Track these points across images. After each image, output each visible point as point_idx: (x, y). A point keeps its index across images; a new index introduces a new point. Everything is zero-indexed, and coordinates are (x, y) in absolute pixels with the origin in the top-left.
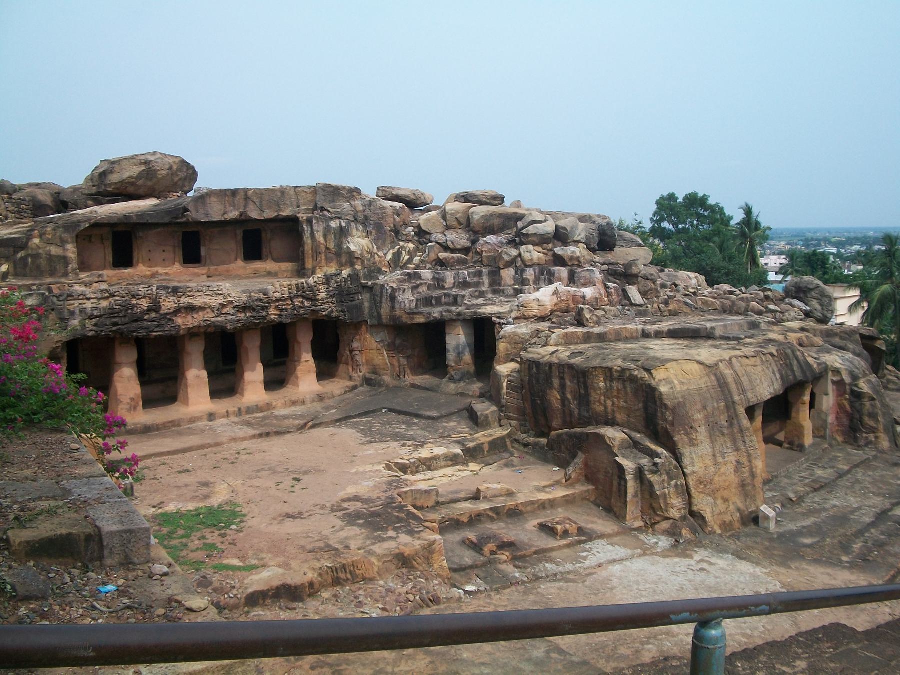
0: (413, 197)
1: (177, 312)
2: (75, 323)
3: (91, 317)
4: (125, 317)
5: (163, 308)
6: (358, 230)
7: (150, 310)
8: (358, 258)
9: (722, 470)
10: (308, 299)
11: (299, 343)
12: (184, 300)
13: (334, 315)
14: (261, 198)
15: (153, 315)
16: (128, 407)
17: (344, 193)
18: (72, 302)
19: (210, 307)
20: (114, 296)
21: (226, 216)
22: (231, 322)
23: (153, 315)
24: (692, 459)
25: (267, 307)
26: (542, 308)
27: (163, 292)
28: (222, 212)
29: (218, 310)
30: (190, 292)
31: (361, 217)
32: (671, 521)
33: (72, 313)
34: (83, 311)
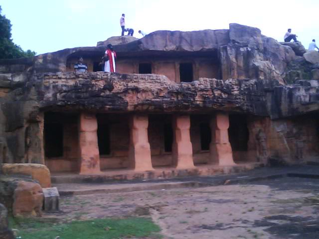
1: (126, 91)
4: (86, 92)
5: (115, 88)
6: (260, 56)
7: (105, 89)
10: (225, 93)
11: (219, 129)
12: (130, 84)
15: (108, 93)
16: (89, 164)
18: (48, 80)
19: (151, 91)
20: (79, 77)
21: (167, 48)
22: (167, 102)
23: (108, 93)
27: (116, 78)
28: (164, 45)
29: (157, 93)
30: (136, 79)
31: (262, 48)
33: (47, 88)
34: (55, 87)
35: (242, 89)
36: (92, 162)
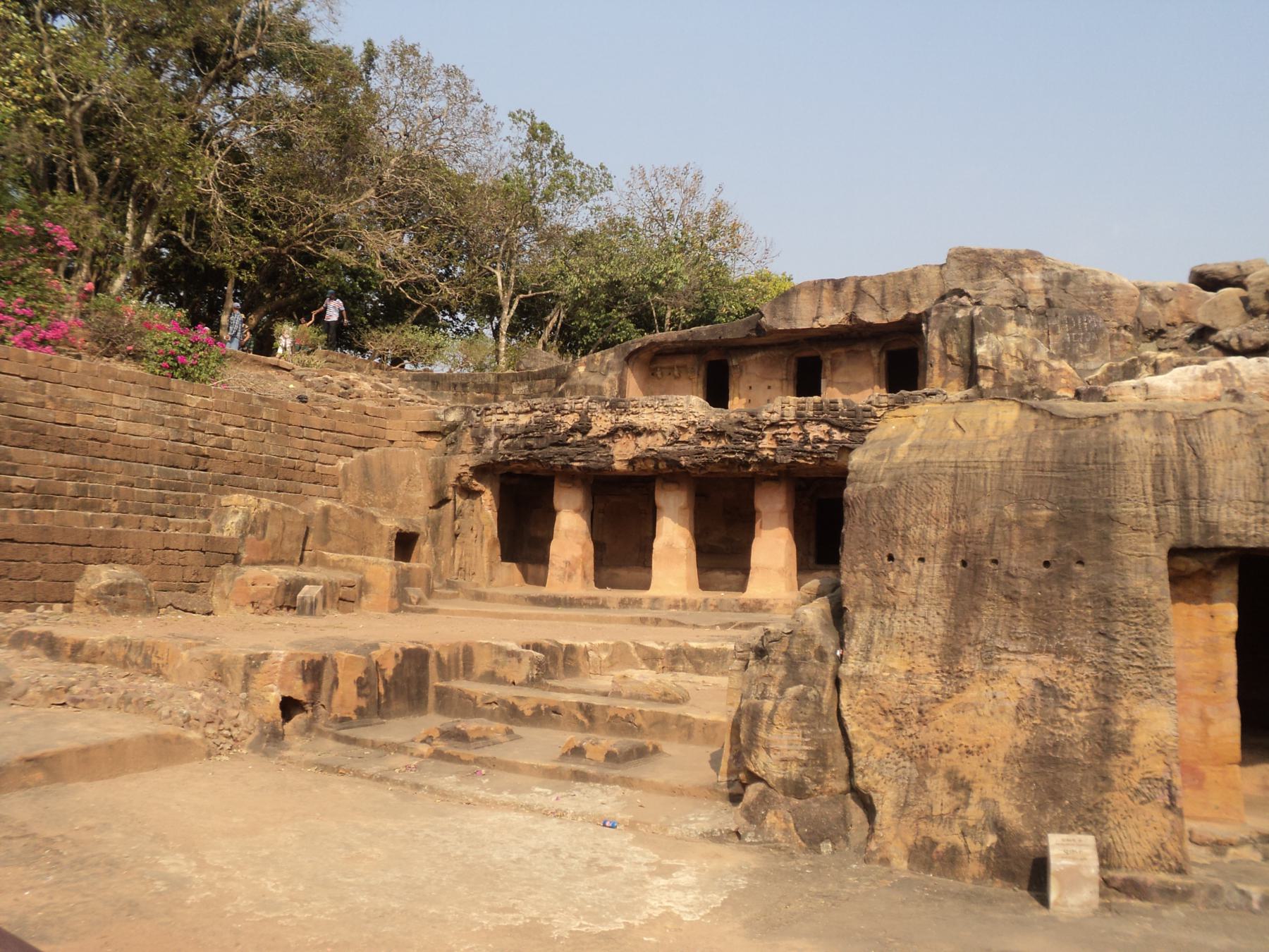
1: (612, 434)
2: (489, 444)
3: (503, 436)
7: (574, 429)
8: (986, 368)
9: (970, 695)
10: (842, 429)
12: (622, 419)
14: (883, 290)
16: (561, 573)
17: (1000, 260)
19: (661, 431)
22: (687, 454)
23: (579, 437)
24: (870, 641)
25: (755, 436)
27: (598, 407)
29: (672, 434)
33: (487, 432)
34: (497, 430)
36: (568, 569)
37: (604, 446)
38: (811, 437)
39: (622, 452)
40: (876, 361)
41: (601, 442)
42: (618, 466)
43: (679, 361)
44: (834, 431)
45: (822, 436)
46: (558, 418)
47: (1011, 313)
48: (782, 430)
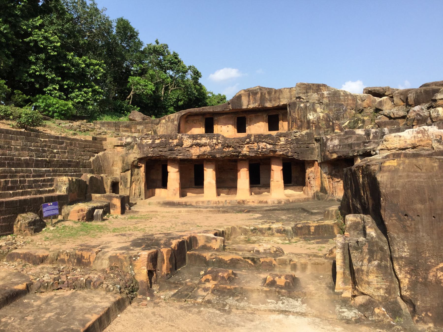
0: (382, 90)
1: (191, 146)
7: (177, 145)
10: (270, 144)
12: (194, 141)
13: (290, 154)
23: (179, 148)
25: (242, 147)
26: (402, 142)
32: (368, 297)
35: (290, 140)
36: (174, 192)
37: (188, 150)
38: (260, 147)
39: (195, 152)
40: (265, 119)
41: (187, 149)
42: (194, 157)
43: (196, 118)
44: (267, 145)
45: (263, 147)
46: (171, 141)
47: (318, 105)
48: (250, 145)
